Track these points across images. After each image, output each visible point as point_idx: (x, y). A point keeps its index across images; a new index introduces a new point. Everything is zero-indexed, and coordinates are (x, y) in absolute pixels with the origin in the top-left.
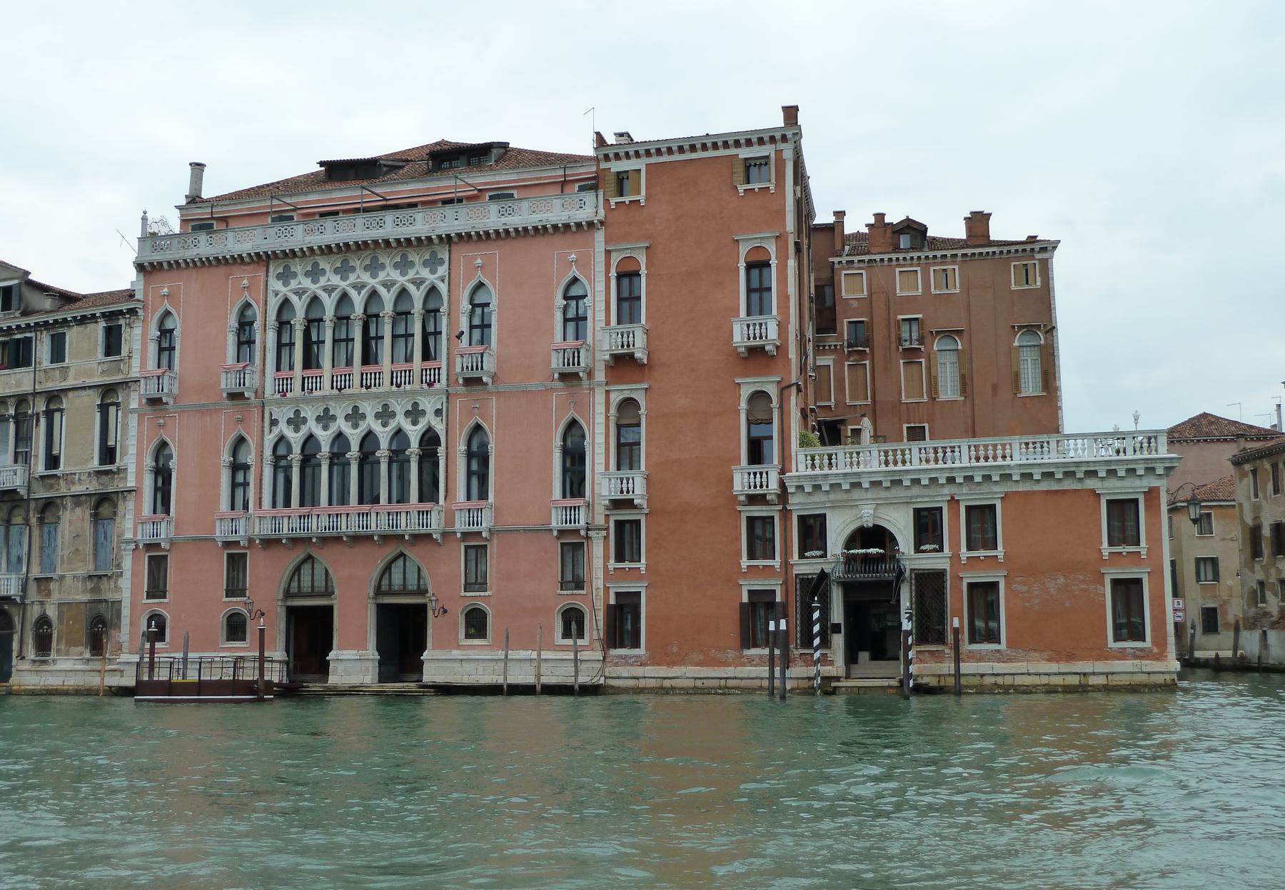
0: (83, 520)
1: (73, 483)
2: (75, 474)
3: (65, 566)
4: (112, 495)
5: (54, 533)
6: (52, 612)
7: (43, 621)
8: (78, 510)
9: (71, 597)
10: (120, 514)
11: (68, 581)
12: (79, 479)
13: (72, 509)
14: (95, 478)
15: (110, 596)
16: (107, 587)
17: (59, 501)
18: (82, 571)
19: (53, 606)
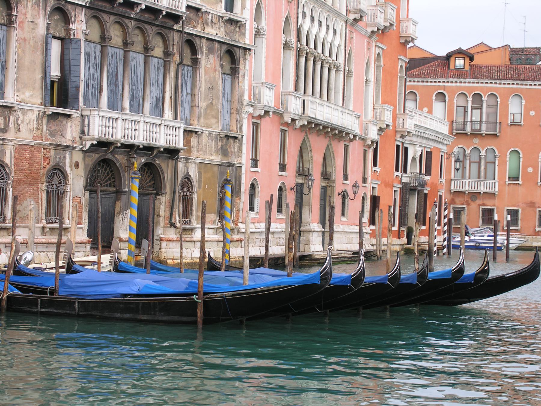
0: (215, 70)
1: (207, 24)
2: (208, 13)
3: (202, 120)
4: (236, 49)
5: (186, 78)
6: (193, 172)
7: (187, 181)
8: (211, 57)
9: (213, 158)
10: (241, 73)
11: (205, 138)
12: (212, 22)
13: (207, 55)
14: (222, 24)
15: (234, 160)
16: (233, 150)
17: (197, 41)
18: (217, 128)
19: (194, 165)
